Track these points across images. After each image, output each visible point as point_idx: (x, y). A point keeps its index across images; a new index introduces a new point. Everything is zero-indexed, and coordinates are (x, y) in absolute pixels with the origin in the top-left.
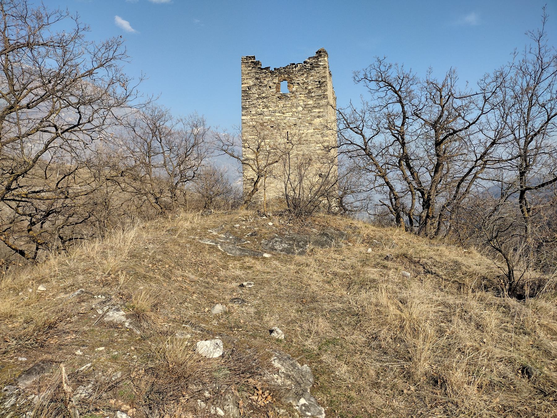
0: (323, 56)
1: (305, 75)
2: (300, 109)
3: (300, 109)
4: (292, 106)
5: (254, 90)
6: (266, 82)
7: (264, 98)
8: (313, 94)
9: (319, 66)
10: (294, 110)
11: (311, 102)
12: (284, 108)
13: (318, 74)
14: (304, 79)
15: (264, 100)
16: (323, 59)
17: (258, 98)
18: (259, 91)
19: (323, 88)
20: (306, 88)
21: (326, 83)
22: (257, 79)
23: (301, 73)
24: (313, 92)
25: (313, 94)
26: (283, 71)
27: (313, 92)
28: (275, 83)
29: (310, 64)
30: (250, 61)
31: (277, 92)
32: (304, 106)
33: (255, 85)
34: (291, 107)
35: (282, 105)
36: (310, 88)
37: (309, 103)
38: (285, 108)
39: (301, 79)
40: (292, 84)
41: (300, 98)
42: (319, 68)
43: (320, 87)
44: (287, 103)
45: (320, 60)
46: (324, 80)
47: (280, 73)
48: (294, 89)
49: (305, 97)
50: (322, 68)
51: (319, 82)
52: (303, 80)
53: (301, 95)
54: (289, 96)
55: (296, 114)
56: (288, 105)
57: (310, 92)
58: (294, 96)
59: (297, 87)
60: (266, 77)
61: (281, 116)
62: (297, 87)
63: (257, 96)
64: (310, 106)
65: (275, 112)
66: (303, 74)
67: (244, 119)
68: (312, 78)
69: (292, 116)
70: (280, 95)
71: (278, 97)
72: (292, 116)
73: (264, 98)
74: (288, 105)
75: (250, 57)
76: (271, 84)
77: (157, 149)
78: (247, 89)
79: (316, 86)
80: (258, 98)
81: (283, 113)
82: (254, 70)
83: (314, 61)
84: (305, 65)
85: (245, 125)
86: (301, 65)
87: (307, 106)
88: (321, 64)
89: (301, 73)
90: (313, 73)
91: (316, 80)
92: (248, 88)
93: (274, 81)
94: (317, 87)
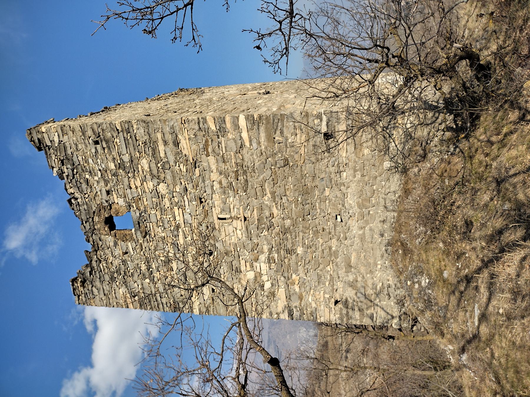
0: (40, 136)
1: (87, 176)
2: (162, 188)
3: (162, 188)
4: (158, 206)
5: (136, 287)
6: (116, 262)
7: (149, 268)
8: (126, 158)
9: (62, 145)
10: (166, 203)
11: (144, 163)
12: (167, 226)
13: (80, 147)
14: (96, 178)
15: (154, 266)
16: (45, 136)
17: (152, 280)
18: (136, 275)
19: (109, 135)
20: (114, 175)
21: (95, 127)
22: (113, 279)
23: (84, 186)
24: (121, 159)
25: (126, 158)
26: (87, 226)
27: (121, 159)
28: (116, 244)
29: (63, 165)
30: (81, 289)
31: (132, 239)
32: (156, 181)
33: (125, 283)
34: (163, 211)
35: (159, 230)
36: (112, 166)
37: (146, 167)
38: (166, 222)
39: (100, 187)
40: (110, 205)
41: (139, 190)
42: (67, 144)
43: (107, 142)
44: (153, 219)
45: (49, 144)
46: (89, 133)
47: (93, 231)
48: (121, 202)
49: (134, 176)
50: (66, 137)
51: (96, 143)
52: (98, 182)
53: (133, 186)
54: (138, 214)
55: (176, 200)
56: (159, 217)
57: (121, 166)
58: (136, 202)
59: (115, 196)
60: (106, 260)
61: (183, 231)
62: (115, 196)
63: (147, 280)
64: (153, 165)
65: (175, 245)
66: (87, 181)
67: (200, 310)
68: (90, 161)
69: (182, 207)
70: (139, 233)
71: (145, 237)
72: (182, 207)
73: (149, 268)
74: (159, 217)
75: (74, 289)
76: (118, 252)
77: (284, 389)
78: (136, 298)
79: (106, 151)
80: (152, 280)
81: (178, 227)
82: (98, 283)
83: (53, 157)
84: (68, 176)
85: (211, 309)
86: (68, 187)
87: (155, 172)
88: (56, 139)
89: (84, 186)
90: (80, 158)
91: (93, 151)
92: (134, 297)
93: (112, 244)
94: (109, 148)
